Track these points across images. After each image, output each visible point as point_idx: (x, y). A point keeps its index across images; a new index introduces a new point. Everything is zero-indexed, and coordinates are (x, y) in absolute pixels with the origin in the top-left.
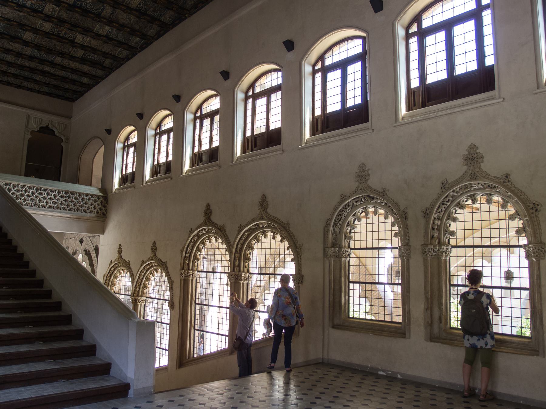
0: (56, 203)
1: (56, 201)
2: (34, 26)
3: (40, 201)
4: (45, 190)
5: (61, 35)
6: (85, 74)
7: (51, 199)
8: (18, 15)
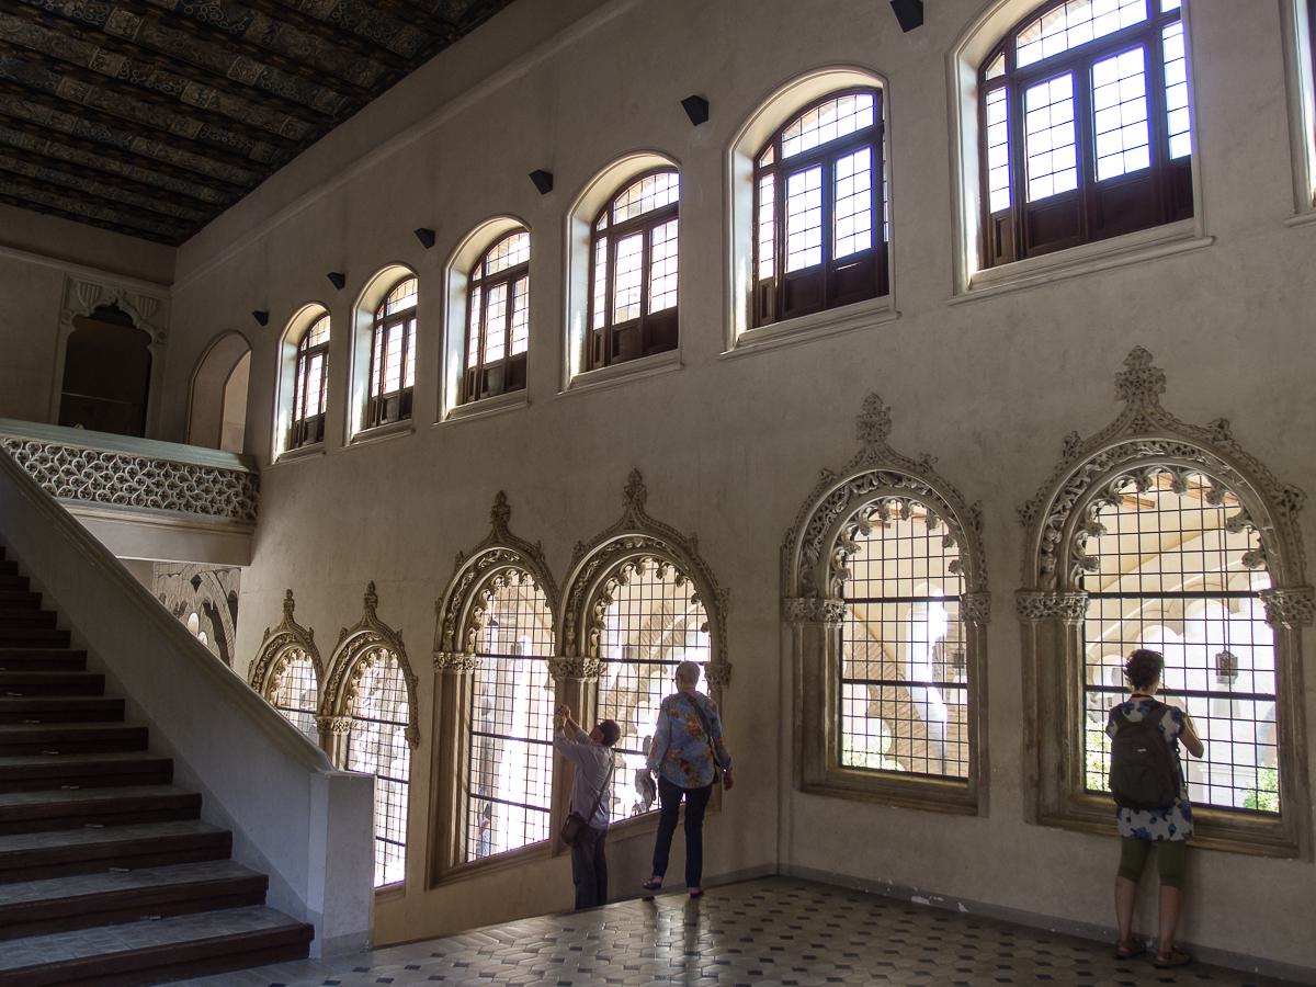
0: (136, 490)
1: (134, 484)
3: (96, 485)
4: (109, 458)
5: (147, 84)
6: (204, 179)
7: (122, 480)
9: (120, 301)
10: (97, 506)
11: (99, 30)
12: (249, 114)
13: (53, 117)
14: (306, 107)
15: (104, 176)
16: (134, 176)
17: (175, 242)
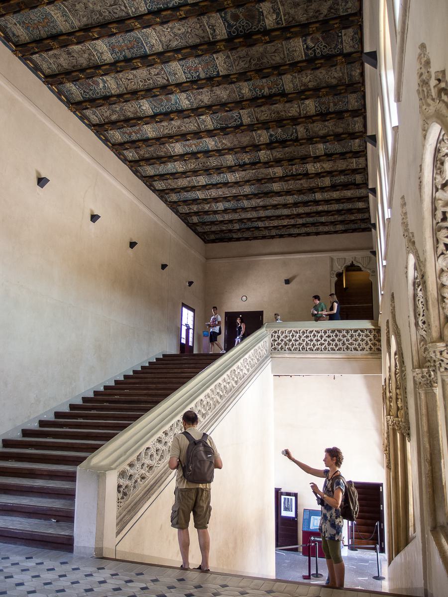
0: (324, 344)
1: (323, 342)
2: (269, 177)
3: (307, 344)
4: (311, 332)
6: (349, 200)
7: (317, 340)
8: (252, 173)
9: (354, 262)
10: (308, 353)
11: (259, 162)
12: (338, 166)
13: (284, 200)
14: (351, 152)
15: (319, 213)
16: (330, 209)
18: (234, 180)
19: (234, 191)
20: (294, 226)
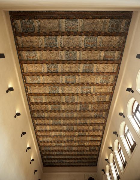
6: (93, 155)
15: (83, 159)
17: (96, 165)
18: (64, 145)
19: (62, 149)
20: (75, 162)
